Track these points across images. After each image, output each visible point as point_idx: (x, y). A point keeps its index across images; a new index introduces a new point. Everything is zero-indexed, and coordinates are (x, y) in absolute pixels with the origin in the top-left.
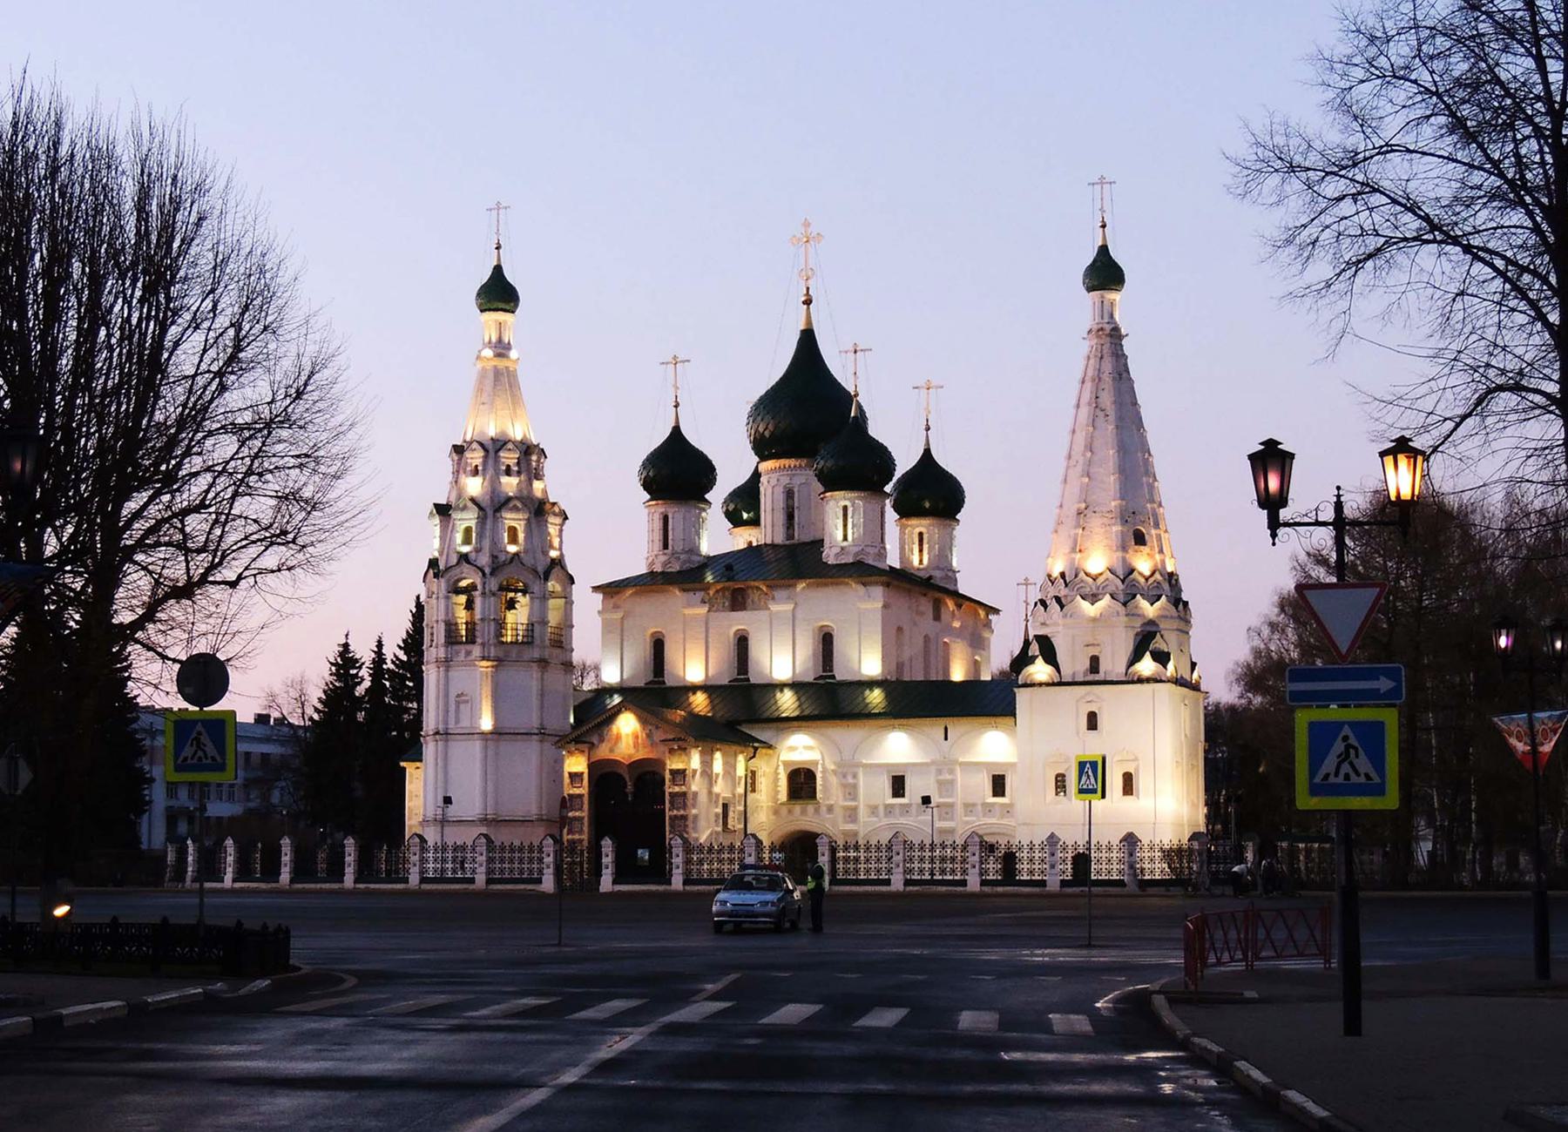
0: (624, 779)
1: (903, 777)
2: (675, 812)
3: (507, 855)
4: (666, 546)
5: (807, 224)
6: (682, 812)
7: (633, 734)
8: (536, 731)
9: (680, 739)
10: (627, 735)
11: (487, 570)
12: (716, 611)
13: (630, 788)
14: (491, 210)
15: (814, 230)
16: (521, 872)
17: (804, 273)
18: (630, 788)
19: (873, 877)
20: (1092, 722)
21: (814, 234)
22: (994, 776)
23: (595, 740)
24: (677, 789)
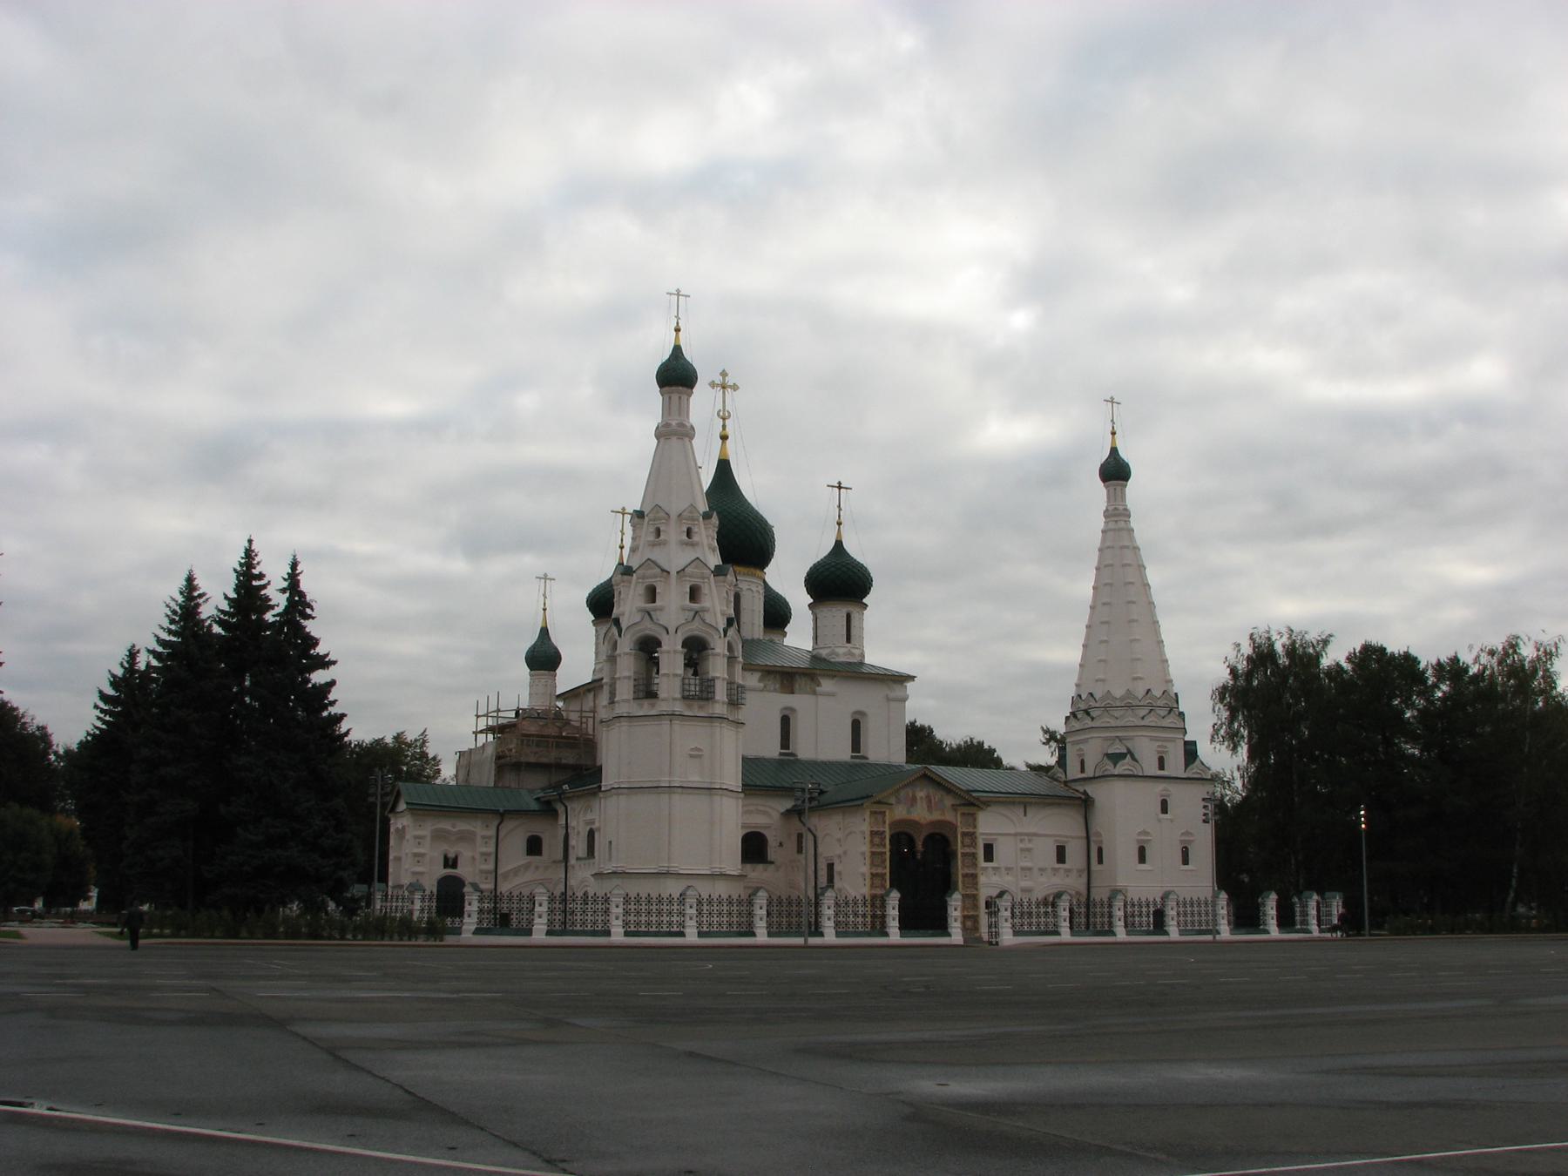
2: (966, 871)
3: (632, 907)
5: (724, 374)
6: (972, 871)
10: (921, 798)
12: (769, 691)
13: (919, 846)
14: (671, 294)
15: (730, 381)
16: (649, 924)
17: (721, 414)
18: (919, 846)
19: (643, 929)
20: (1164, 808)
21: (731, 383)
22: (1058, 847)
23: (892, 800)
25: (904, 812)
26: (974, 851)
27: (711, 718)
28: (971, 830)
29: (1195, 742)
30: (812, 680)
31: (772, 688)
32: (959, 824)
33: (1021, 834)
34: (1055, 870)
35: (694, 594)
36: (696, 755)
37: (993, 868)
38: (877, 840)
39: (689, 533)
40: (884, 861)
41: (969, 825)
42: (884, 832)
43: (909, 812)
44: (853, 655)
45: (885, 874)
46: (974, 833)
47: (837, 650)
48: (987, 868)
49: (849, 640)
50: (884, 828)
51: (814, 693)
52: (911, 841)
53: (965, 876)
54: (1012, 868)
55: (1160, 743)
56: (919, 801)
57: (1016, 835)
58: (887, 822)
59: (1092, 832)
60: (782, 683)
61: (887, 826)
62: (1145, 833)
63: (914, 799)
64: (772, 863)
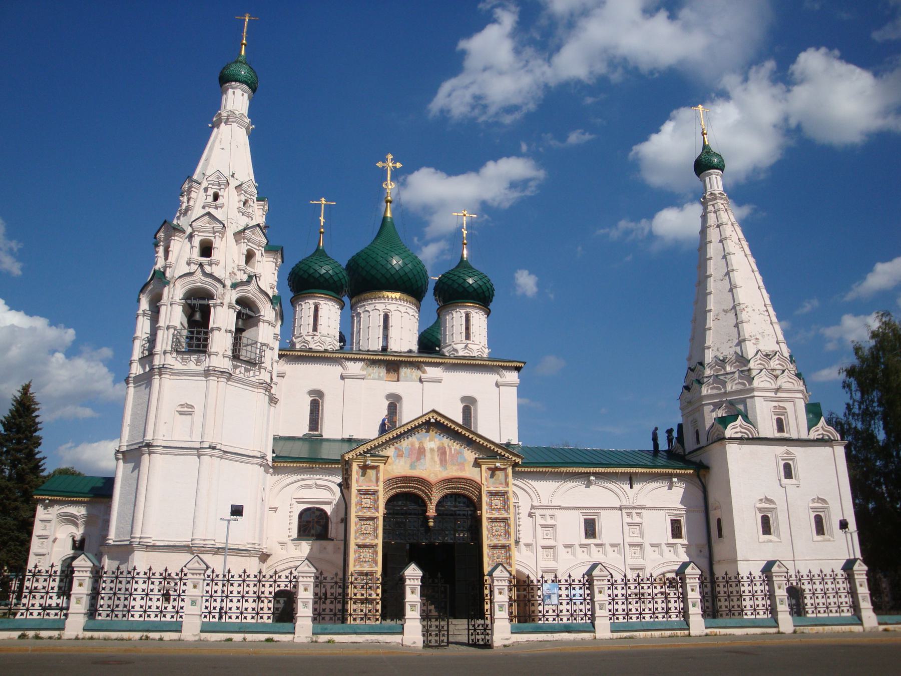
0: (424, 505)
1: (594, 520)
2: (495, 542)
4: (315, 329)
6: (503, 541)
7: (439, 448)
8: (258, 455)
9: (502, 457)
10: (432, 450)
11: (228, 283)
12: (374, 379)
13: (432, 511)
18: (432, 511)
20: (788, 472)
24: (496, 515)
25: (408, 466)
26: (505, 515)
27: (207, 373)
28: (501, 489)
29: (819, 403)
30: (419, 368)
31: (377, 377)
32: (484, 481)
33: (626, 508)
34: (669, 545)
35: (206, 250)
36: (186, 410)
37: (596, 545)
38: (367, 501)
39: (216, 197)
40: (376, 529)
41: (501, 484)
42: (375, 492)
43: (412, 466)
44: (471, 350)
45: (376, 545)
46: (506, 492)
47: (455, 346)
48: (589, 545)
49: (468, 337)
50: (378, 486)
51: (421, 381)
52: (420, 503)
53: (495, 547)
54: (619, 545)
55: (776, 404)
56: (428, 454)
57: (620, 509)
59: (711, 500)
60: (388, 371)
61: (381, 484)
62: (767, 500)
63: (421, 452)
64: (332, 540)
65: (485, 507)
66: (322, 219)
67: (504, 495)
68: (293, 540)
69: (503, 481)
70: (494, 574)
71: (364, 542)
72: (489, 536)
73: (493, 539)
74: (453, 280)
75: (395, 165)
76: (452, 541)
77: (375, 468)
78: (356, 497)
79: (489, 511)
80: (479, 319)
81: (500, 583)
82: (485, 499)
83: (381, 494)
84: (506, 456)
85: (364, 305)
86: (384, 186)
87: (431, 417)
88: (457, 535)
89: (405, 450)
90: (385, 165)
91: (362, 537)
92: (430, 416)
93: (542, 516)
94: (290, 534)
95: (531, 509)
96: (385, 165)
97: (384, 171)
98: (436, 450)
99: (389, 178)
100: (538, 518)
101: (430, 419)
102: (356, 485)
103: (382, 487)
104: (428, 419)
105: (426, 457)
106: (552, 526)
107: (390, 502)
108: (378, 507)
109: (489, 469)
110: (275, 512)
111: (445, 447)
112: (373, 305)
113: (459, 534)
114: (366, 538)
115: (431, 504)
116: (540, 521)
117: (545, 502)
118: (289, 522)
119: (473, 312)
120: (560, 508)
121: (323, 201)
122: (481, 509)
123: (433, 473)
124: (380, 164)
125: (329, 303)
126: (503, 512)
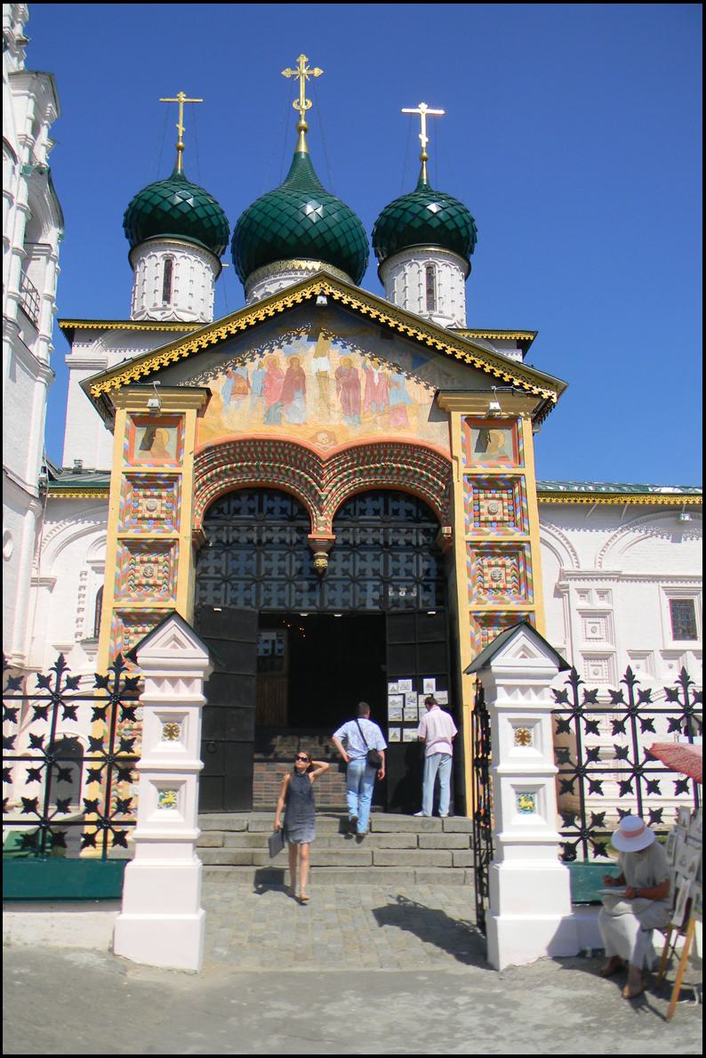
0: (300, 515)
2: (490, 605)
4: (167, 297)
7: (339, 373)
10: (322, 376)
18: (322, 528)
24: (491, 535)
26: (517, 536)
32: (458, 451)
38: (152, 504)
40: (171, 573)
41: (504, 458)
42: (173, 479)
43: (269, 417)
48: (681, 653)
50: (180, 464)
56: (312, 387)
58: (189, 447)
61: (188, 462)
63: (296, 380)
65: (461, 516)
66: (181, 128)
67: (512, 488)
68: (83, 642)
69: (509, 452)
70: (497, 664)
71: (138, 605)
72: (475, 590)
73: (484, 598)
74: (402, 209)
75: (311, 72)
76: (377, 608)
77: (175, 421)
78: (124, 494)
79: (472, 526)
80: (449, 276)
81: (520, 701)
82: (462, 494)
83: (187, 484)
84: (516, 383)
85: (263, 285)
86: (295, 105)
87: (317, 293)
88: (391, 594)
89: (253, 379)
90: (295, 73)
91: (134, 595)
92: (317, 289)
93: (583, 593)
94: (79, 630)
95: (560, 580)
96: (295, 73)
97: (294, 82)
98: (332, 376)
99: (302, 93)
100: (574, 595)
101: (314, 297)
102: (124, 462)
103: (191, 466)
104: (308, 297)
105: (307, 395)
106: (603, 614)
107: (214, 511)
108: (178, 516)
109: (472, 421)
110: (51, 589)
111: (356, 370)
112: (278, 284)
113: (397, 590)
114: (147, 595)
115: (321, 510)
116: (579, 603)
117: (587, 565)
118: (77, 606)
119: (440, 264)
120: (619, 577)
121: (182, 97)
122: (451, 523)
123: (325, 431)
124: (287, 73)
125: (193, 258)
126: (511, 530)
